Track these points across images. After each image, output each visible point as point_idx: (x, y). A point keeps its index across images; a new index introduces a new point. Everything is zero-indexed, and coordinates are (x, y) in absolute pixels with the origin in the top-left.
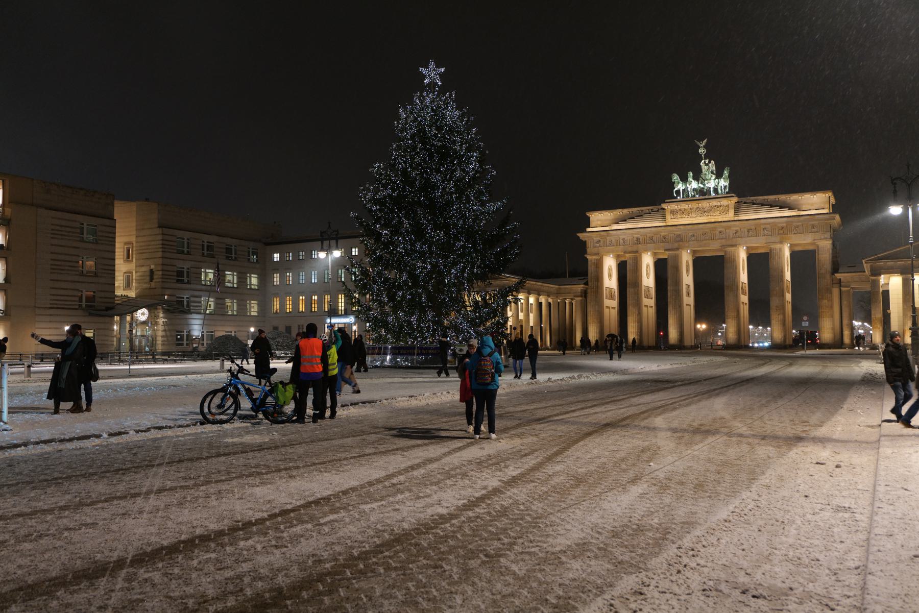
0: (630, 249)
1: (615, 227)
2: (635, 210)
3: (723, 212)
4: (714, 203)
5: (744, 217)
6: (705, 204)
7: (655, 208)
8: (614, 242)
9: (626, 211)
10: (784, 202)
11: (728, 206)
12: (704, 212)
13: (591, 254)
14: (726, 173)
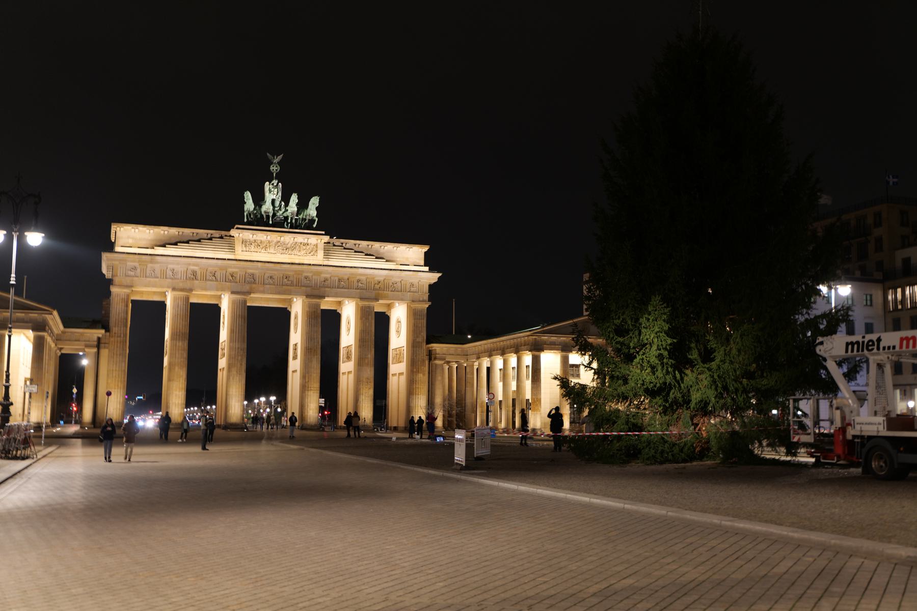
0: (181, 285)
1: (160, 251)
2: (188, 231)
3: (309, 251)
4: (300, 238)
6: (288, 239)
7: (216, 233)
8: (158, 272)
9: (174, 231)
10: (377, 251)
11: (316, 245)
12: (287, 248)
13: (121, 286)
14: (314, 202)
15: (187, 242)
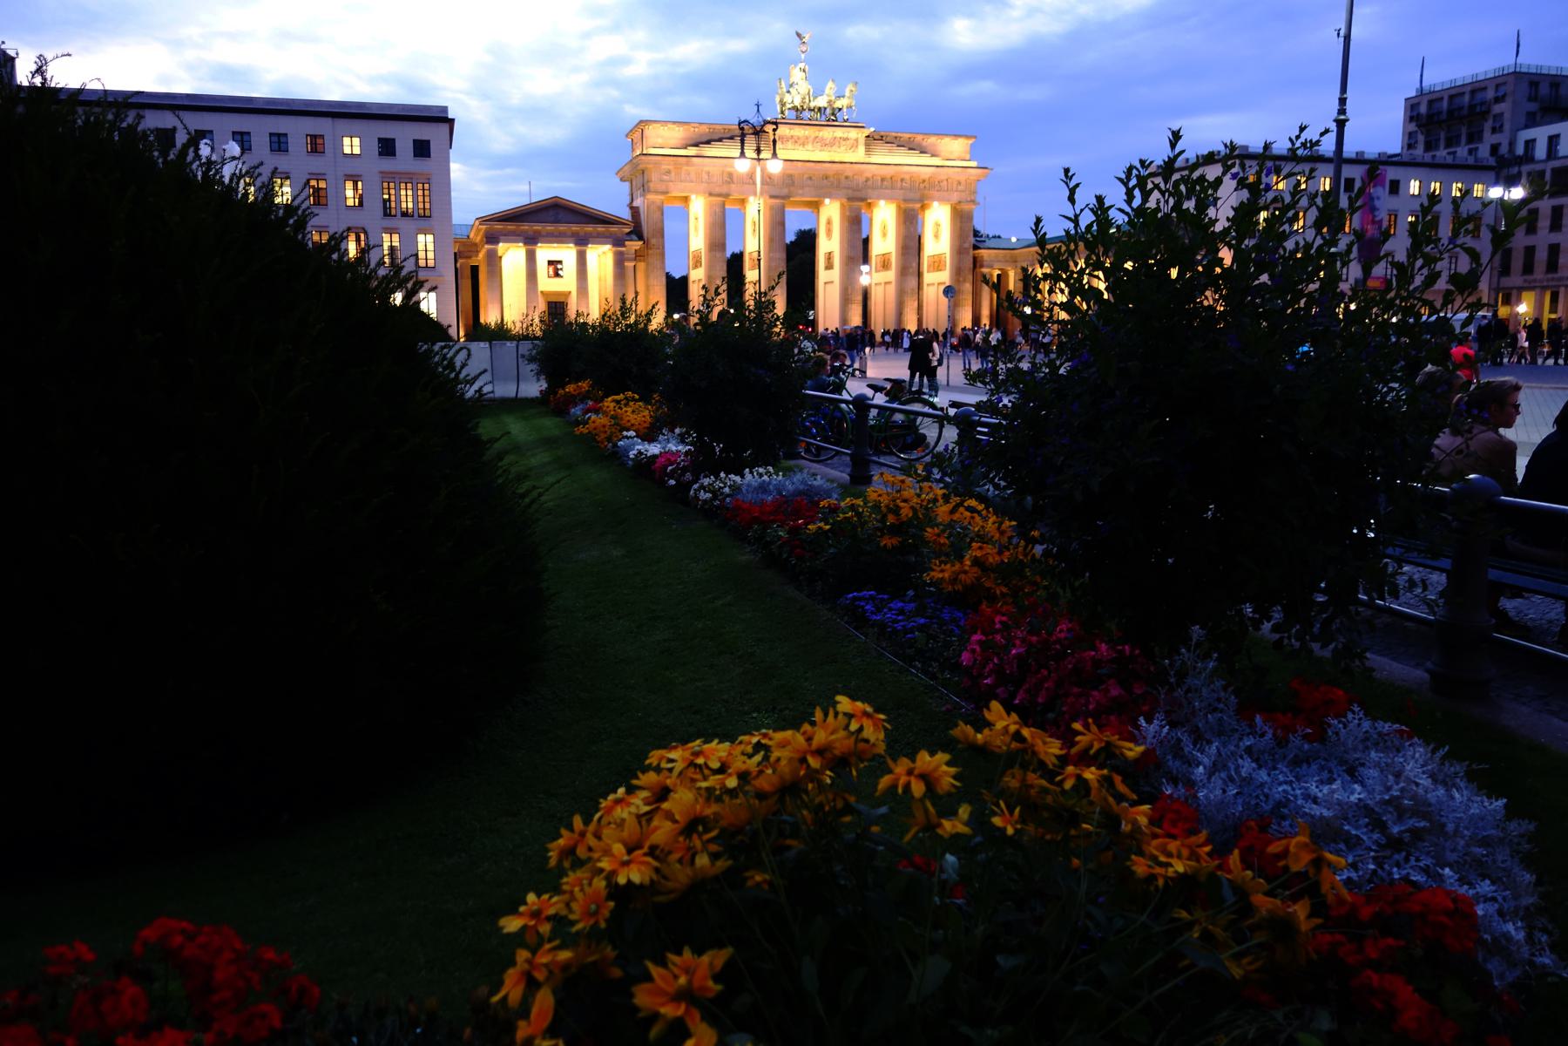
0: (717, 190)
1: (692, 151)
5: (874, 159)
6: (827, 133)
8: (693, 176)
12: (827, 144)
13: (657, 192)
15: (720, 140)
